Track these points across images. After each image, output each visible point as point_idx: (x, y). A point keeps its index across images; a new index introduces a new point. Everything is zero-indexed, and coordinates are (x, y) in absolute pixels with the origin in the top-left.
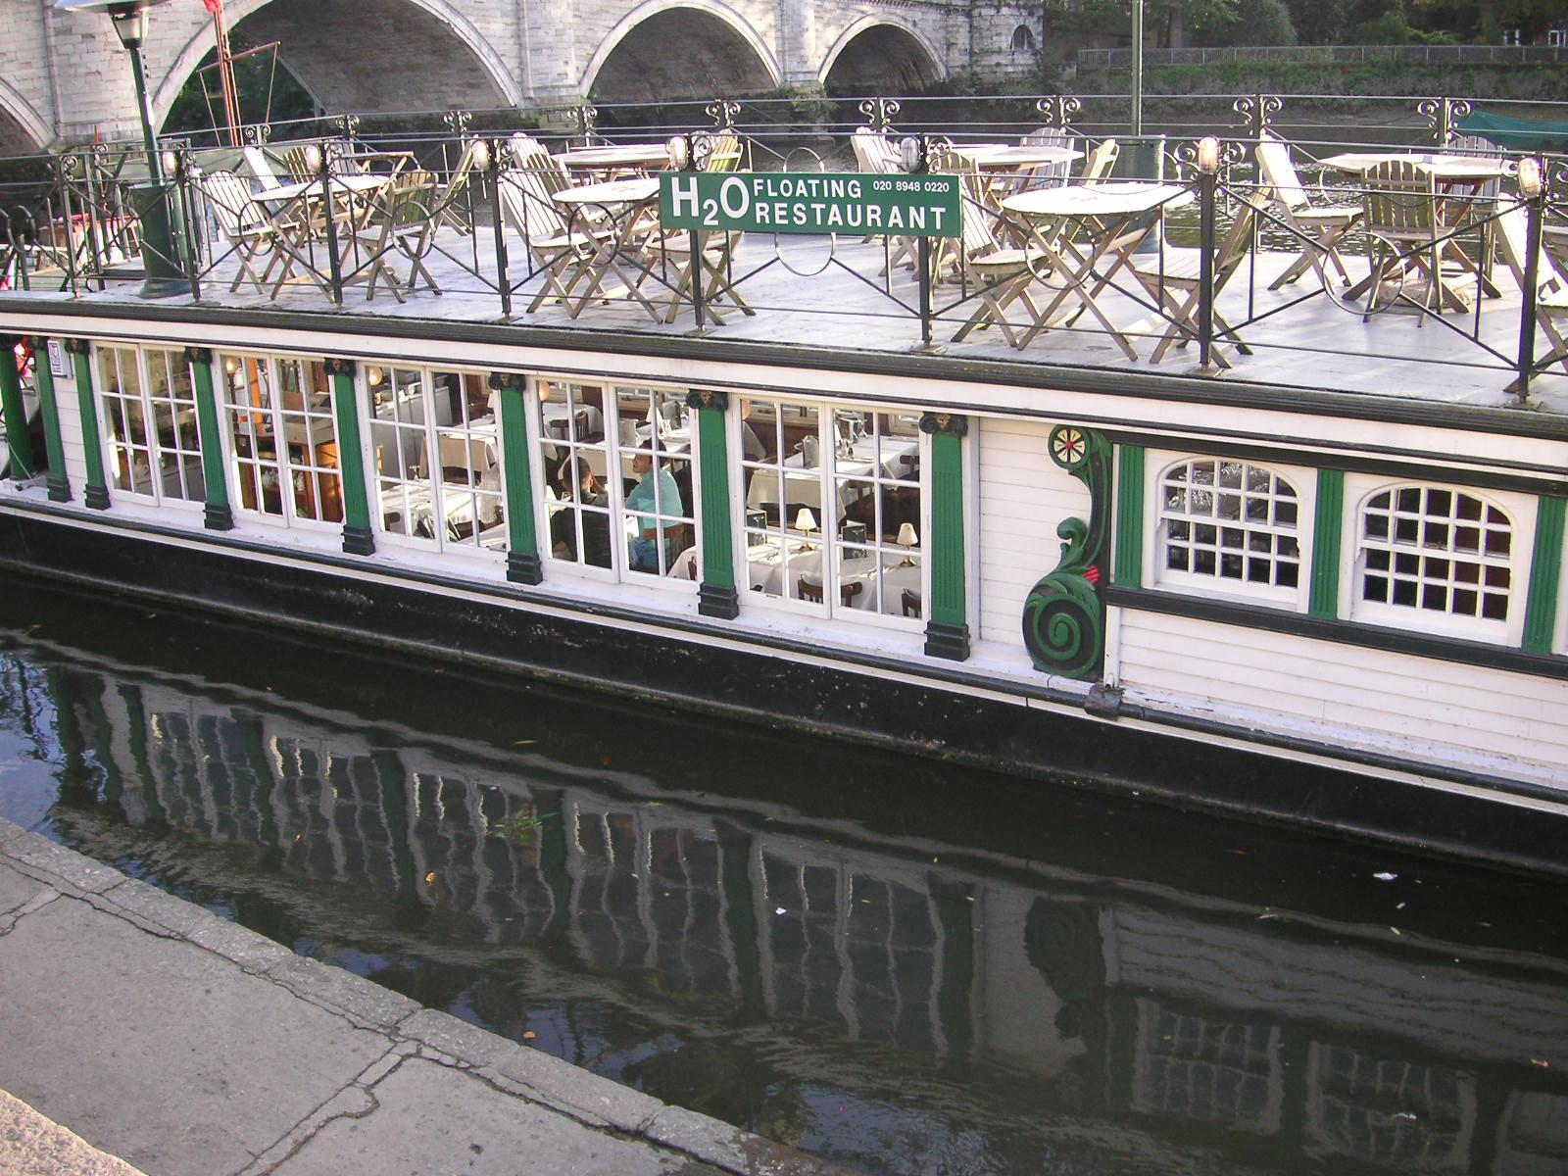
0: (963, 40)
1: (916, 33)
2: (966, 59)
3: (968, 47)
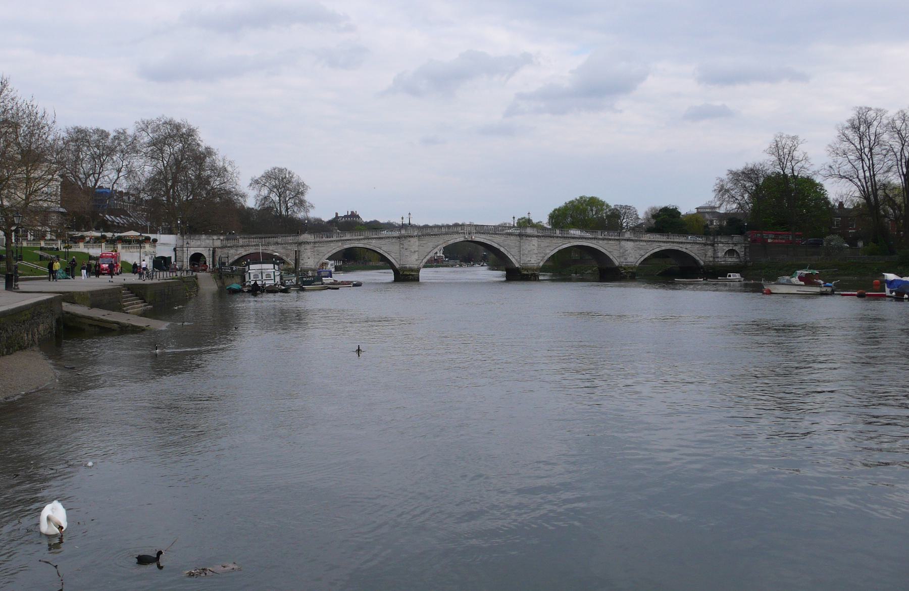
0: (710, 253)
1: (687, 251)
2: (711, 259)
3: (712, 255)
